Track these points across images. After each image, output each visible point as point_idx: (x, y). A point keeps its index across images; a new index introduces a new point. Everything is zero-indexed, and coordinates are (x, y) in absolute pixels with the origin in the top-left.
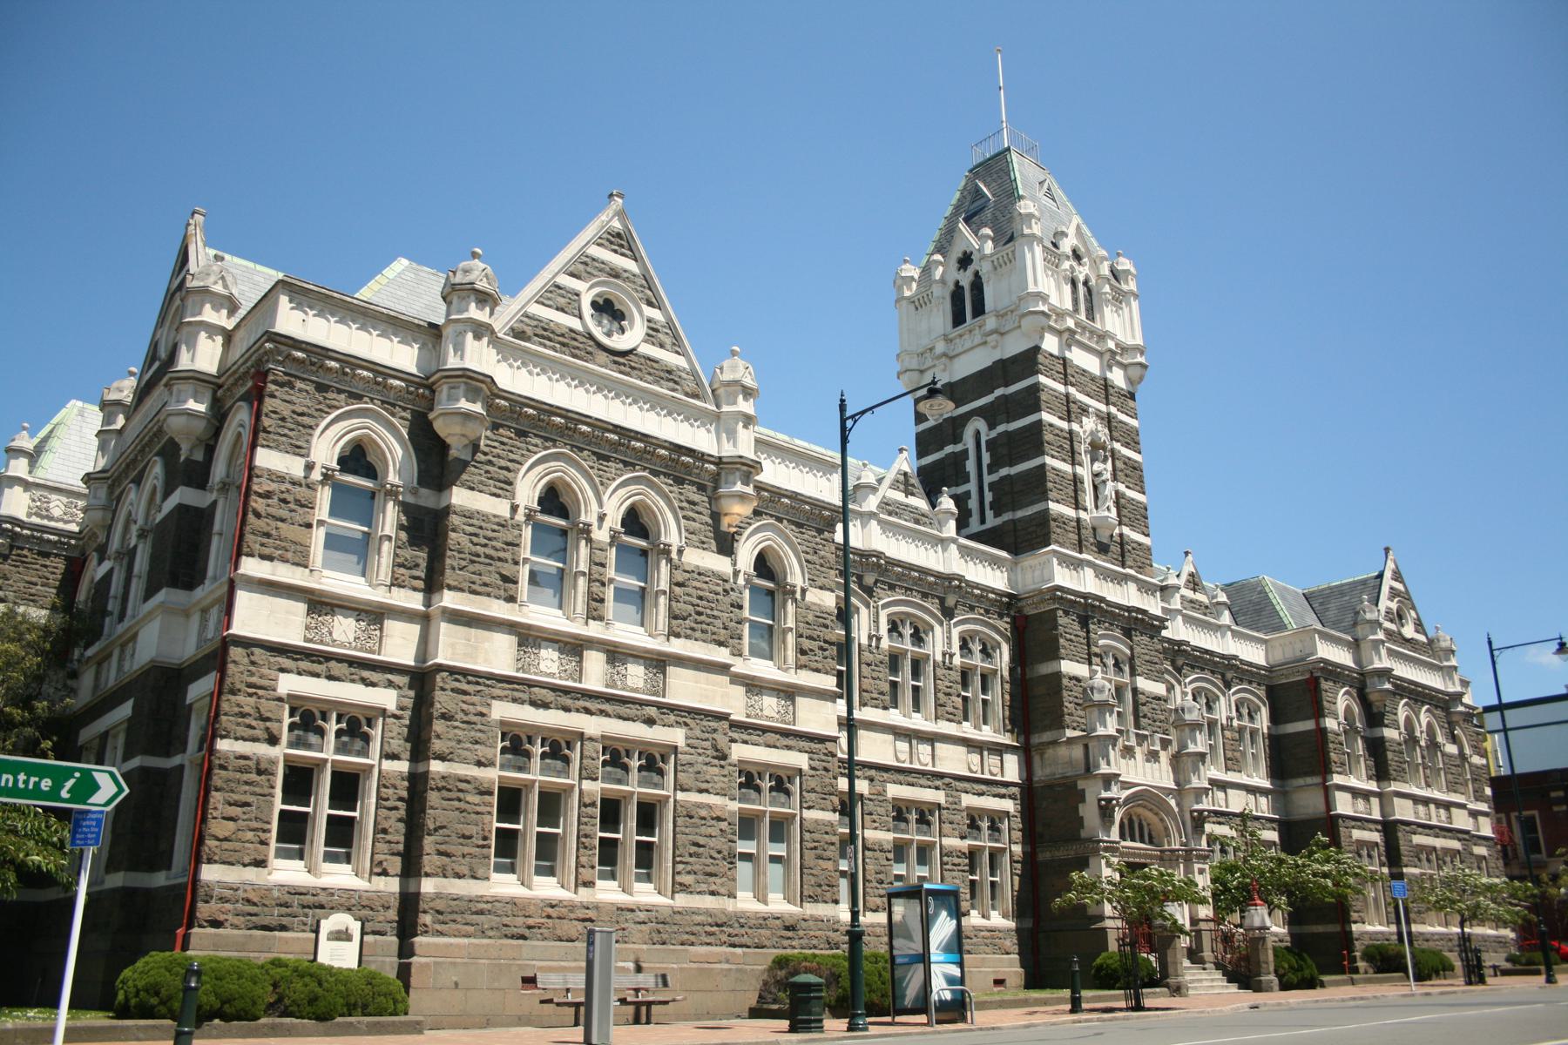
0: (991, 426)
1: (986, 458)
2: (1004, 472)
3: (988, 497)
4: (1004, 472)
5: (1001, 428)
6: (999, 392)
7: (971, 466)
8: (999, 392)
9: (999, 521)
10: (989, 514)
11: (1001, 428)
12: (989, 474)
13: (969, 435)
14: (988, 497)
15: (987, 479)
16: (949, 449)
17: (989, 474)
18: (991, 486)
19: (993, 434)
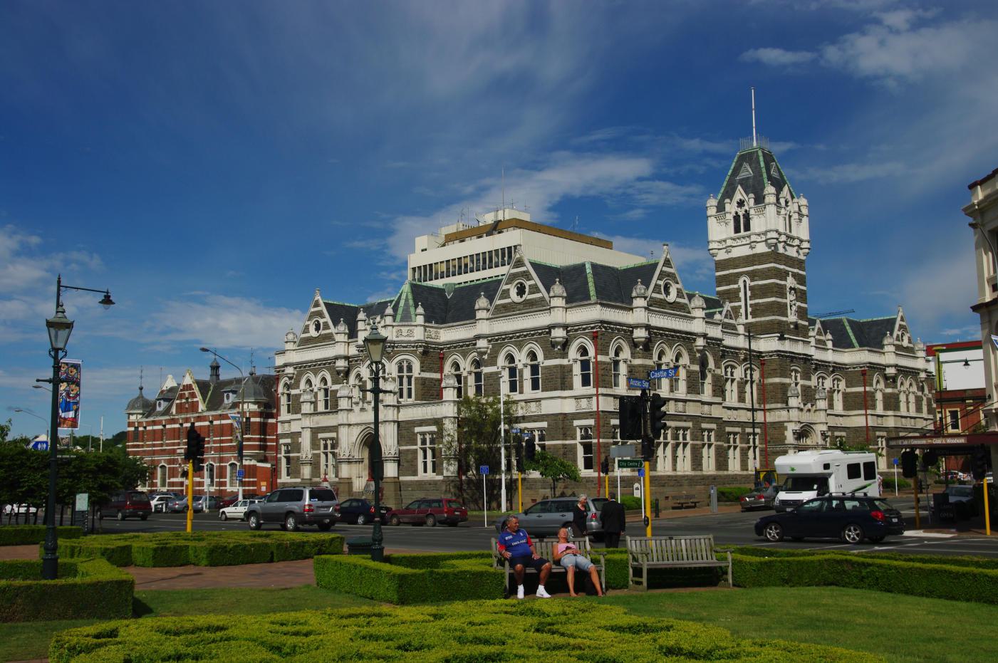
0: (752, 281)
1: (749, 293)
2: (757, 301)
3: (749, 310)
4: (757, 301)
5: (756, 283)
6: (756, 267)
7: (742, 295)
8: (756, 267)
9: (754, 320)
10: (750, 316)
11: (756, 283)
12: (750, 300)
13: (741, 284)
14: (749, 310)
15: (749, 302)
16: (732, 286)
17: (750, 300)
18: (751, 305)
19: (752, 284)
